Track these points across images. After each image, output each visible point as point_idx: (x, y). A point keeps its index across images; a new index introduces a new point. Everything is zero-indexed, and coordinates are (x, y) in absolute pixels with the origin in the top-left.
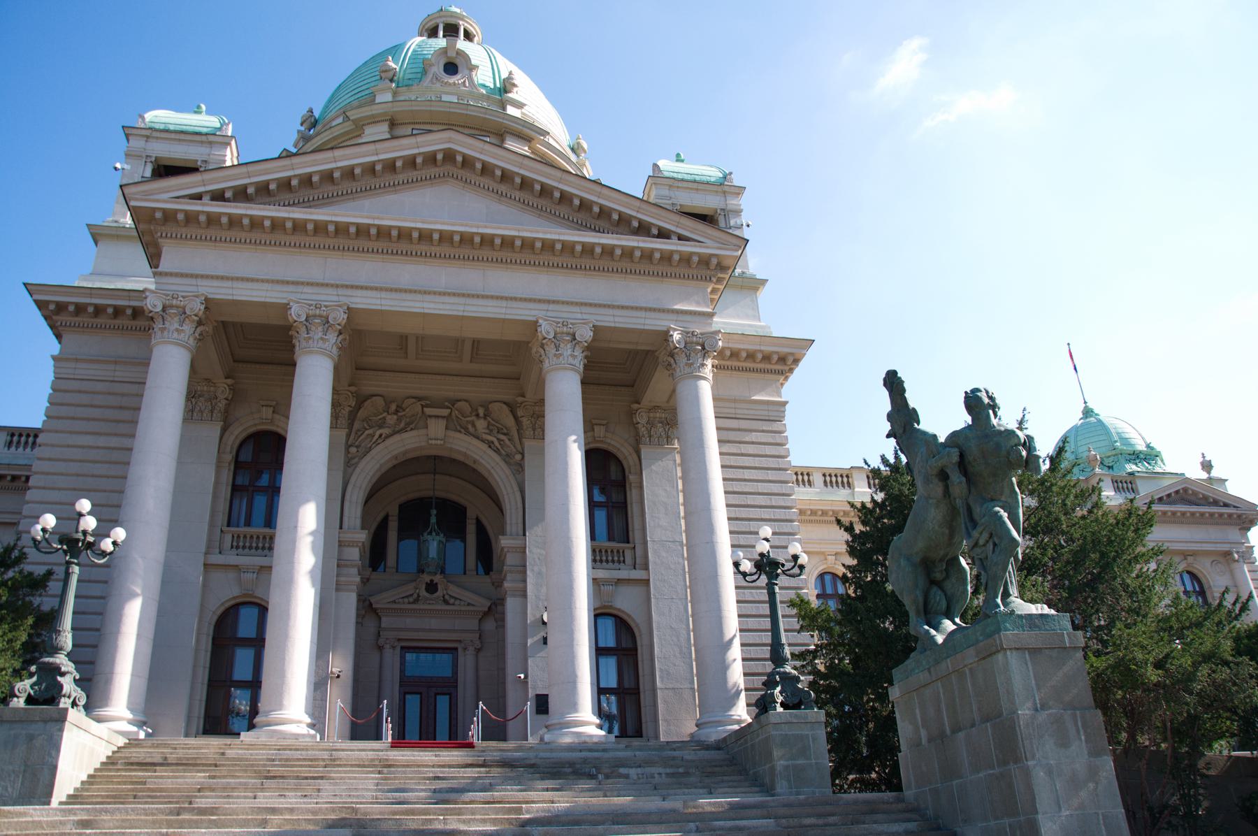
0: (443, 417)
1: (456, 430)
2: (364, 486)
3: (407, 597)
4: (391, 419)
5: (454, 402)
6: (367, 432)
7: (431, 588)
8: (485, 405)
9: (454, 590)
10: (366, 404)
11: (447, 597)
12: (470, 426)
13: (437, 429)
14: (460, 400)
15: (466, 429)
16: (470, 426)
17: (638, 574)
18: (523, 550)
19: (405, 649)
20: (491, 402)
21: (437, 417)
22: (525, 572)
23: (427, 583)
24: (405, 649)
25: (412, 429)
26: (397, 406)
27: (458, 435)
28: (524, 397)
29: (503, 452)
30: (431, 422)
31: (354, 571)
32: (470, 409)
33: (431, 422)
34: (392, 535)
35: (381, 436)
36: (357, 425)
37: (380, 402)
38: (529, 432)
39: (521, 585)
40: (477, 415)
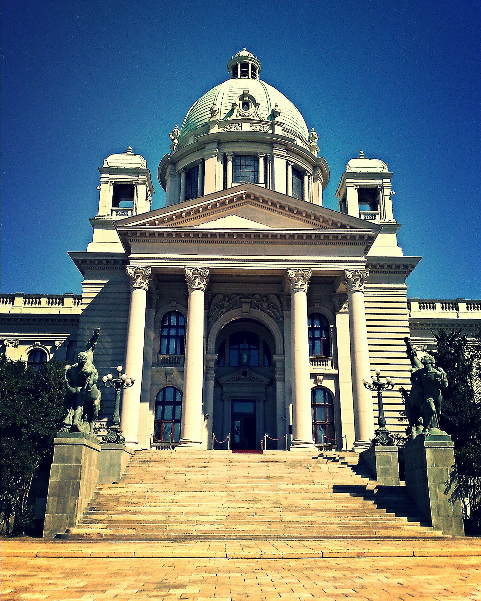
0: (249, 302)
1: (255, 308)
2: (216, 334)
3: (234, 378)
4: (226, 304)
5: (253, 295)
6: (216, 311)
7: (245, 374)
8: (267, 296)
9: (254, 375)
10: (216, 298)
11: (251, 378)
12: (260, 306)
13: (246, 307)
14: (255, 294)
15: (258, 307)
16: (260, 306)
17: (335, 372)
18: (283, 361)
19: (234, 401)
20: (269, 294)
21: (246, 302)
22: (284, 371)
23: (242, 372)
24: (234, 401)
25: (235, 308)
26: (229, 298)
27: (255, 310)
28: (283, 292)
29: (274, 317)
30: (243, 305)
31: (213, 372)
32: (260, 298)
33: (244, 305)
34: (227, 350)
35: (222, 312)
36: (212, 307)
37: (221, 296)
38: (286, 308)
39: (282, 376)
40: (263, 301)
